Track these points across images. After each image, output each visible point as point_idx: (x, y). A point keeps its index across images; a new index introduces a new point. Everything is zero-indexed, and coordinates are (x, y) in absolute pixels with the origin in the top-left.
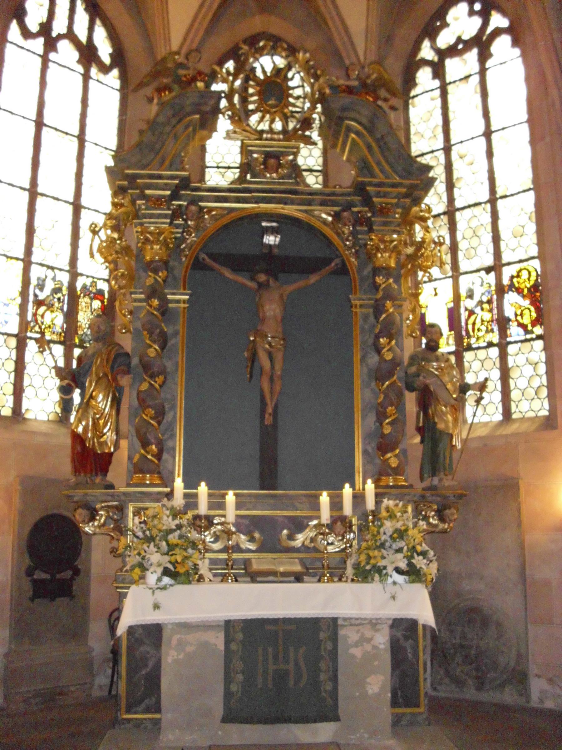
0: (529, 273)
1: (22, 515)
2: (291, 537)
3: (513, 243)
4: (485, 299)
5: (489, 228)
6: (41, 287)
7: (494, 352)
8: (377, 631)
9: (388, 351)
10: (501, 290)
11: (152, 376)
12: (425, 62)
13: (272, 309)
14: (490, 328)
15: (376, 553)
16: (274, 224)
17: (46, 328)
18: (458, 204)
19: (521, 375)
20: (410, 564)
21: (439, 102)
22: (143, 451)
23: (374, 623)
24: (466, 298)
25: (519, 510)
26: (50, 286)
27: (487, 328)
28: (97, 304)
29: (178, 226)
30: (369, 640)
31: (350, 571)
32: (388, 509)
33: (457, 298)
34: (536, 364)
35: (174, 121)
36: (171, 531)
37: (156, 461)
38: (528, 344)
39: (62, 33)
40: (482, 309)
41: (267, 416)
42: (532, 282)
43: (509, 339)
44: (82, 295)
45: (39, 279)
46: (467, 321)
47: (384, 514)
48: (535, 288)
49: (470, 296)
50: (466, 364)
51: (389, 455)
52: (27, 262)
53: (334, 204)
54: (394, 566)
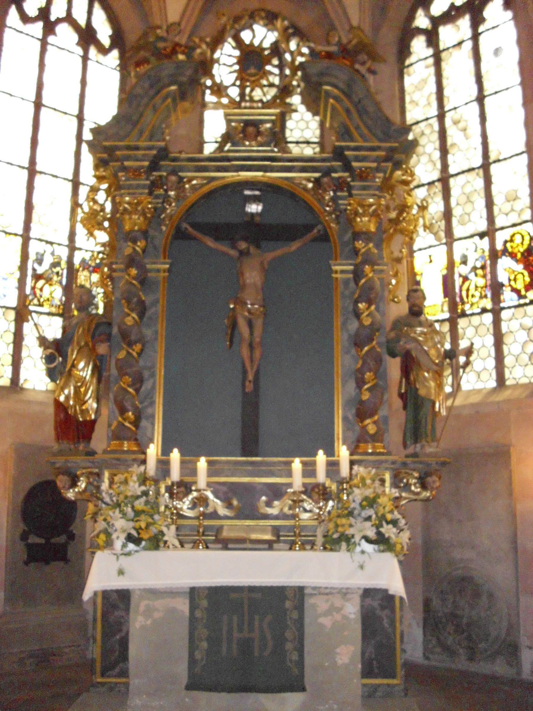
0: (523, 237)
3: (507, 207)
4: (479, 265)
5: (483, 194)
6: (40, 261)
7: (488, 318)
8: (348, 600)
9: (367, 316)
10: (494, 255)
11: (130, 344)
12: (419, 31)
13: (252, 276)
14: (483, 293)
15: (344, 521)
16: (257, 193)
17: (45, 301)
18: (452, 170)
19: (515, 341)
20: (379, 534)
21: (432, 70)
22: (120, 419)
23: (345, 593)
24: (460, 264)
25: (510, 478)
26: (48, 260)
27: (481, 293)
29: (157, 197)
30: (339, 610)
33: (451, 265)
34: (529, 329)
35: (152, 92)
37: (134, 429)
38: (521, 309)
39: (60, 17)
40: (476, 275)
41: (247, 383)
42: (525, 247)
43: (502, 305)
44: (81, 269)
45: (37, 254)
46: (461, 287)
48: (529, 252)
49: (464, 262)
50: (460, 331)
51: (368, 421)
52: (26, 239)
53: (314, 170)
54: (362, 534)
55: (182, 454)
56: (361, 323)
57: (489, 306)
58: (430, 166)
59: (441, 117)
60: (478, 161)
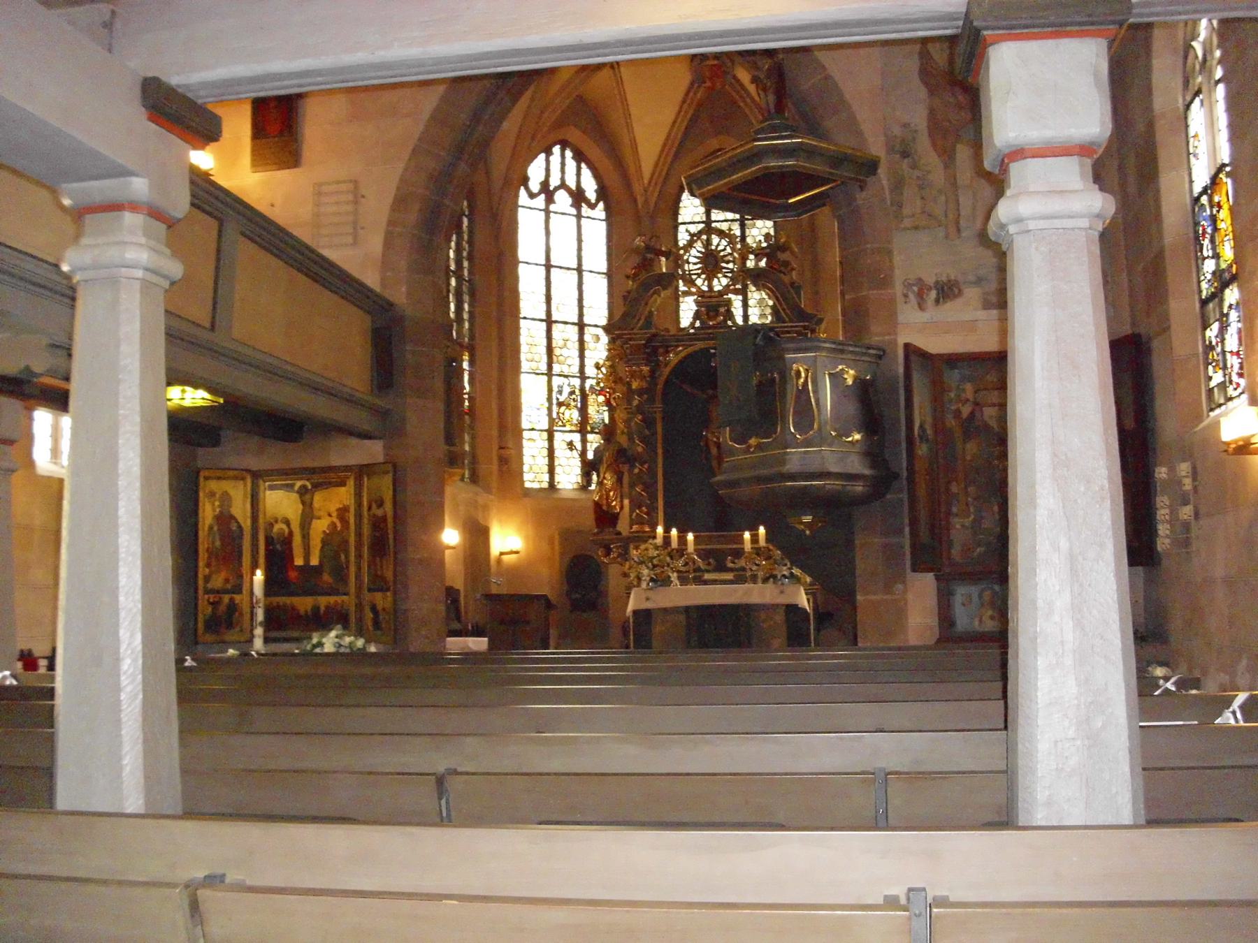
1: (562, 554)
6: (560, 392)
23: (775, 607)
26: (566, 390)
28: (601, 399)
52: (549, 374)
55: (679, 531)
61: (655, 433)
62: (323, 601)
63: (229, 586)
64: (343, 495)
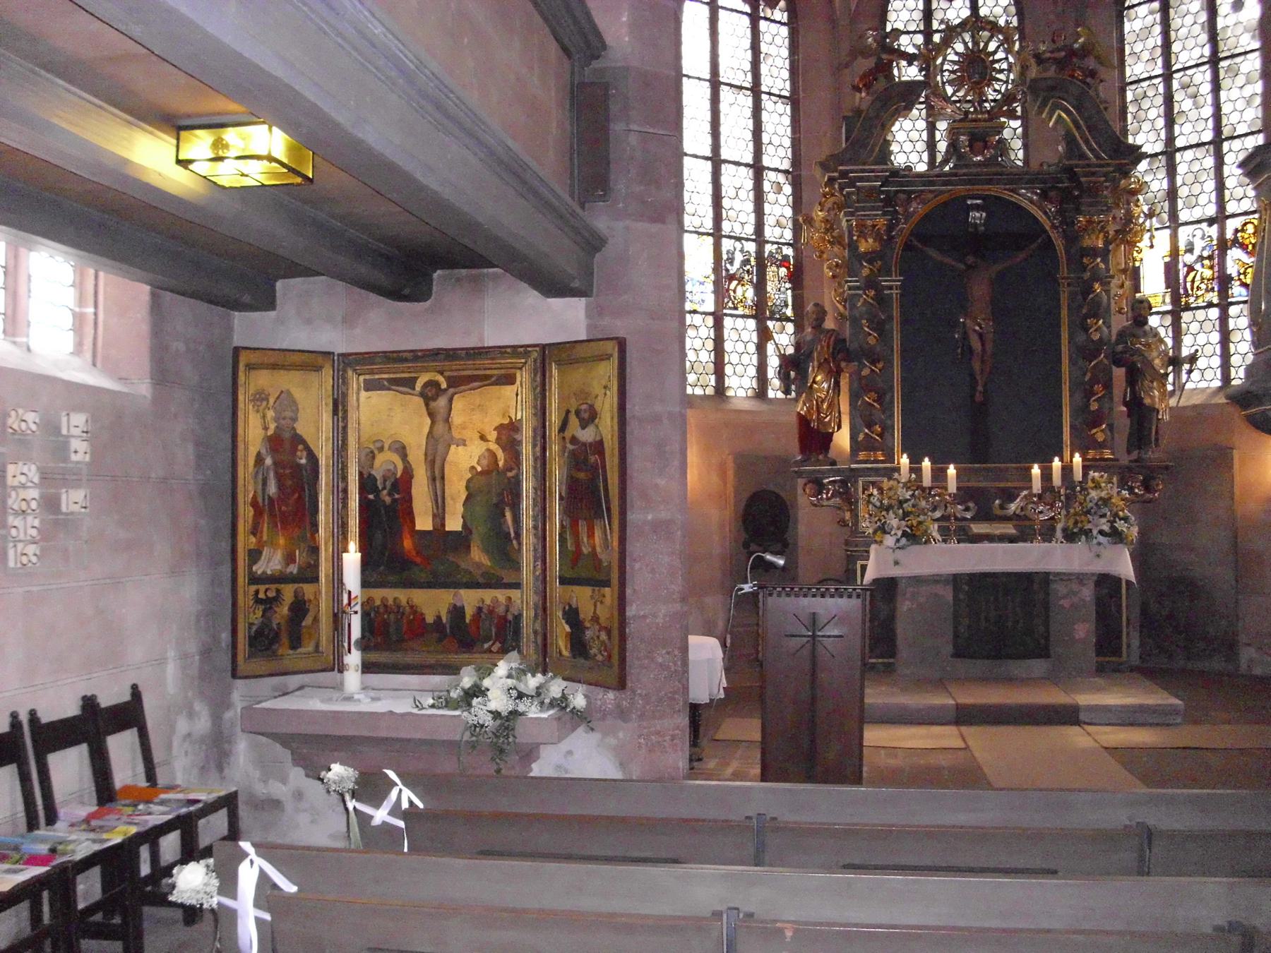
2: (1002, 507)
4: (1206, 254)
7: (1214, 313)
10: (1223, 246)
11: (873, 362)
13: (980, 289)
18: (1180, 143)
20: (1112, 527)
23: (1080, 578)
24: (1186, 252)
26: (739, 258)
28: (783, 271)
30: (1075, 593)
31: (1059, 534)
32: (1093, 480)
33: (1175, 253)
36: (907, 501)
40: (1203, 266)
47: (1090, 484)
49: (1190, 250)
50: (1184, 325)
51: (1094, 431)
55: (933, 462)
56: (1089, 336)
57: (1216, 301)
58: (1152, 136)
59: (1168, 77)
60: (1208, 136)
61: (890, 318)
62: (470, 599)
63: (293, 569)
64: (513, 401)
